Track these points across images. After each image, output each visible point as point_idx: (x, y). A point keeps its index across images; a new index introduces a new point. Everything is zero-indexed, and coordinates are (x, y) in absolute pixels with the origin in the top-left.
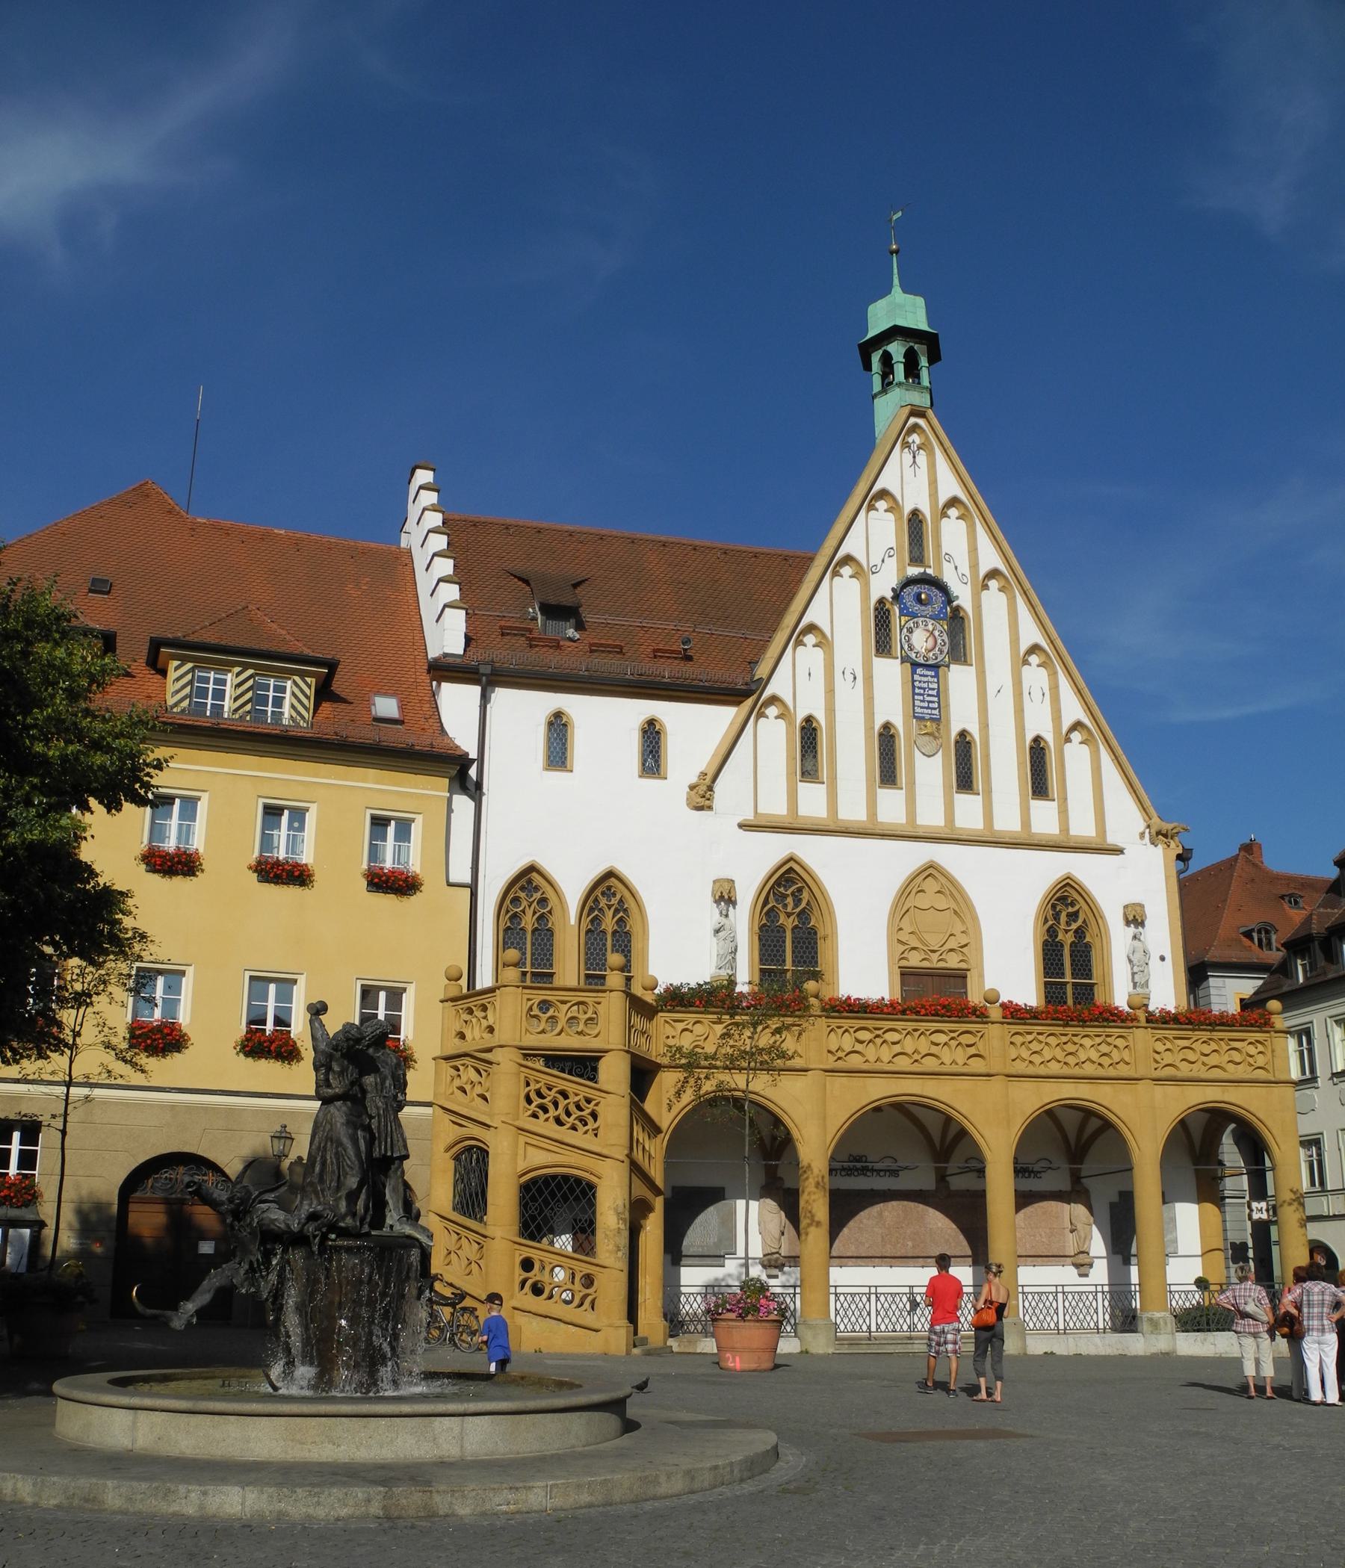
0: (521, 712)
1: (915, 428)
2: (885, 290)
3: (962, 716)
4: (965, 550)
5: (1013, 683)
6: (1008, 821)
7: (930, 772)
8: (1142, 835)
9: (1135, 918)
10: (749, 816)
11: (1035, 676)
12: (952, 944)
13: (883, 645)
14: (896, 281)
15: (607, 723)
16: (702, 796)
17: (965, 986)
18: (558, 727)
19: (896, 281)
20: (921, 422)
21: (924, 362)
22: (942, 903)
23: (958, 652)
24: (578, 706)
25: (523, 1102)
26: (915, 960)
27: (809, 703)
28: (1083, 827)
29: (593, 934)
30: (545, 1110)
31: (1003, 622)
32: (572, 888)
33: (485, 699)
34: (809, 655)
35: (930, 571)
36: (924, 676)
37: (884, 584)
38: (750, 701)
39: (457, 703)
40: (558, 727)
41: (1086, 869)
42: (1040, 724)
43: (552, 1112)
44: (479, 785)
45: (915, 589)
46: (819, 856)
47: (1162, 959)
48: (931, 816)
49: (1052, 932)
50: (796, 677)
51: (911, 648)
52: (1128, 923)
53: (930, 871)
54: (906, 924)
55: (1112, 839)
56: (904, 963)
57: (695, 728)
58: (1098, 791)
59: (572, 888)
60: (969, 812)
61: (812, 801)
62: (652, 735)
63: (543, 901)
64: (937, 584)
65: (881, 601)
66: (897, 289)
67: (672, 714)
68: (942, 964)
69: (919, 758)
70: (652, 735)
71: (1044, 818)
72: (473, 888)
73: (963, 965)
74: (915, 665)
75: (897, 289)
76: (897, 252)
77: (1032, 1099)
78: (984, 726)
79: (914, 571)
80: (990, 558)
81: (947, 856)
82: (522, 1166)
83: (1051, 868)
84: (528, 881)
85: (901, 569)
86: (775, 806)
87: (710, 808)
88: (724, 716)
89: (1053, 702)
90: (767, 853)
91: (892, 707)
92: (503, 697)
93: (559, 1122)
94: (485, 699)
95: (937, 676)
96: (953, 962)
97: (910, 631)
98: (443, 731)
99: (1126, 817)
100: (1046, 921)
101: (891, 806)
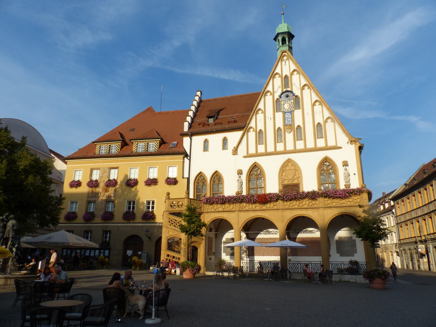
0: (198, 140)
2: (281, 23)
3: (298, 121)
4: (298, 82)
5: (312, 111)
6: (310, 144)
7: (290, 137)
8: (348, 143)
10: (246, 154)
11: (318, 108)
14: (283, 21)
15: (215, 139)
16: (235, 151)
17: (299, 187)
18: (206, 141)
19: (283, 21)
20: (285, 54)
21: (287, 39)
22: (293, 168)
24: (209, 137)
25: (168, 223)
26: (286, 182)
27: (260, 126)
28: (331, 143)
30: (172, 224)
31: (308, 97)
32: (208, 176)
33: (191, 139)
34: (260, 116)
36: (288, 115)
38: (245, 129)
39: (186, 140)
40: (206, 141)
41: (330, 154)
42: (319, 119)
43: (174, 224)
44: (190, 157)
46: (261, 161)
47: (355, 174)
48: (290, 147)
51: (284, 109)
52: (344, 166)
53: (289, 161)
54: (284, 174)
55: (338, 145)
56: (283, 183)
57: (233, 137)
58: (335, 134)
59: (208, 176)
60: (300, 145)
61: (261, 148)
62: (225, 140)
63: (204, 179)
64: (292, 92)
65: (278, 99)
66: (283, 23)
67: (228, 135)
68: (293, 183)
69: (287, 134)
70: (225, 140)
71: (321, 143)
72: (188, 179)
73: (298, 182)
75: (283, 23)
76: (283, 14)
77: (290, 215)
78: (304, 123)
79: (284, 90)
80: (304, 82)
81: (294, 157)
82: (167, 235)
84: (200, 175)
85: (282, 90)
86: (252, 151)
87: (237, 154)
88: (240, 133)
89: (322, 113)
90: (250, 161)
91: (280, 124)
92: (194, 138)
93: (175, 226)
94: (191, 139)
96: (296, 182)
97: (284, 105)
98: (183, 147)
99: (343, 139)
101: (280, 147)
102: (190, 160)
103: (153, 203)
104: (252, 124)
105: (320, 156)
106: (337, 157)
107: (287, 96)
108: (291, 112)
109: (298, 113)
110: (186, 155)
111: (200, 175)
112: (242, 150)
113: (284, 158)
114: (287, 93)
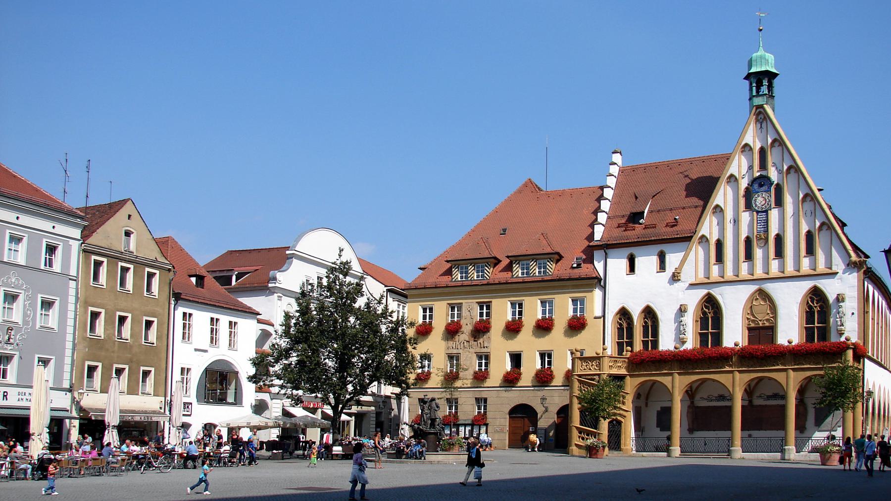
1: (760, 113)
3: (774, 230)
9: (840, 299)
10: (693, 281)
12: (767, 317)
13: (749, 206)
23: (779, 203)
26: (753, 325)
29: (645, 328)
32: (636, 313)
35: (764, 173)
37: (744, 184)
45: (759, 181)
46: (716, 292)
49: (810, 307)
50: (709, 227)
55: (834, 269)
65: (747, 188)
72: (604, 316)
74: (758, 212)
83: (807, 285)
90: (702, 293)
95: (767, 215)
100: (808, 303)
102: (604, 287)
103: (550, 356)
104: (704, 230)
105: (806, 285)
106: (830, 287)
107: (761, 186)
108: (766, 212)
109: (774, 214)
110: (599, 279)
111: (624, 313)
112: (689, 275)
113: (753, 288)
114: (761, 182)
